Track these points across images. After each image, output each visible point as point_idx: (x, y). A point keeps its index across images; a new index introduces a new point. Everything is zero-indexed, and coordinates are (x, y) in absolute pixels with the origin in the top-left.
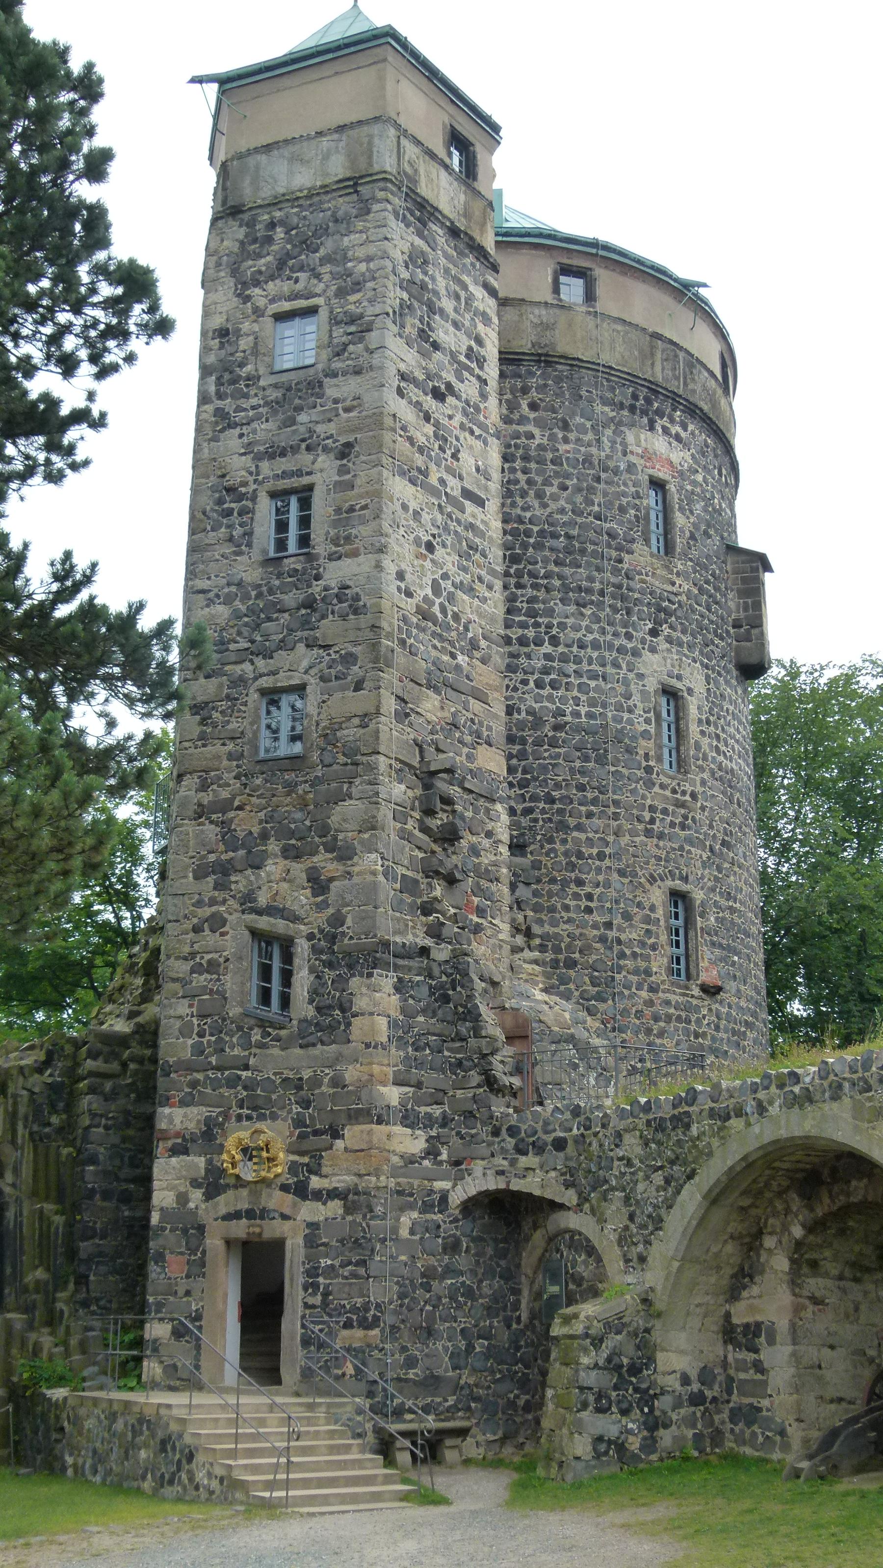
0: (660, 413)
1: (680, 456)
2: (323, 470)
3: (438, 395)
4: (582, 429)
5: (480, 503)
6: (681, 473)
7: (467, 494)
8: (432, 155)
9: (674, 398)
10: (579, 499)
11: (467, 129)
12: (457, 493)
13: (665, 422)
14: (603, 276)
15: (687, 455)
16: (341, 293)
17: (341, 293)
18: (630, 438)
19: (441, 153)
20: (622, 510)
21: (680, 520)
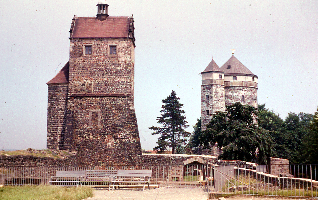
0: (243, 89)
1: (246, 92)
2: (210, 109)
3: (218, 100)
4: (235, 93)
5: (223, 107)
6: (246, 94)
7: (221, 107)
8: (217, 79)
9: (245, 87)
10: (235, 99)
11: (221, 74)
12: (220, 108)
13: (244, 89)
14: (238, 77)
15: (247, 92)
16: (210, 94)
17: (210, 94)
18: (240, 92)
19: (219, 78)
20: (239, 100)
21: (245, 99)
